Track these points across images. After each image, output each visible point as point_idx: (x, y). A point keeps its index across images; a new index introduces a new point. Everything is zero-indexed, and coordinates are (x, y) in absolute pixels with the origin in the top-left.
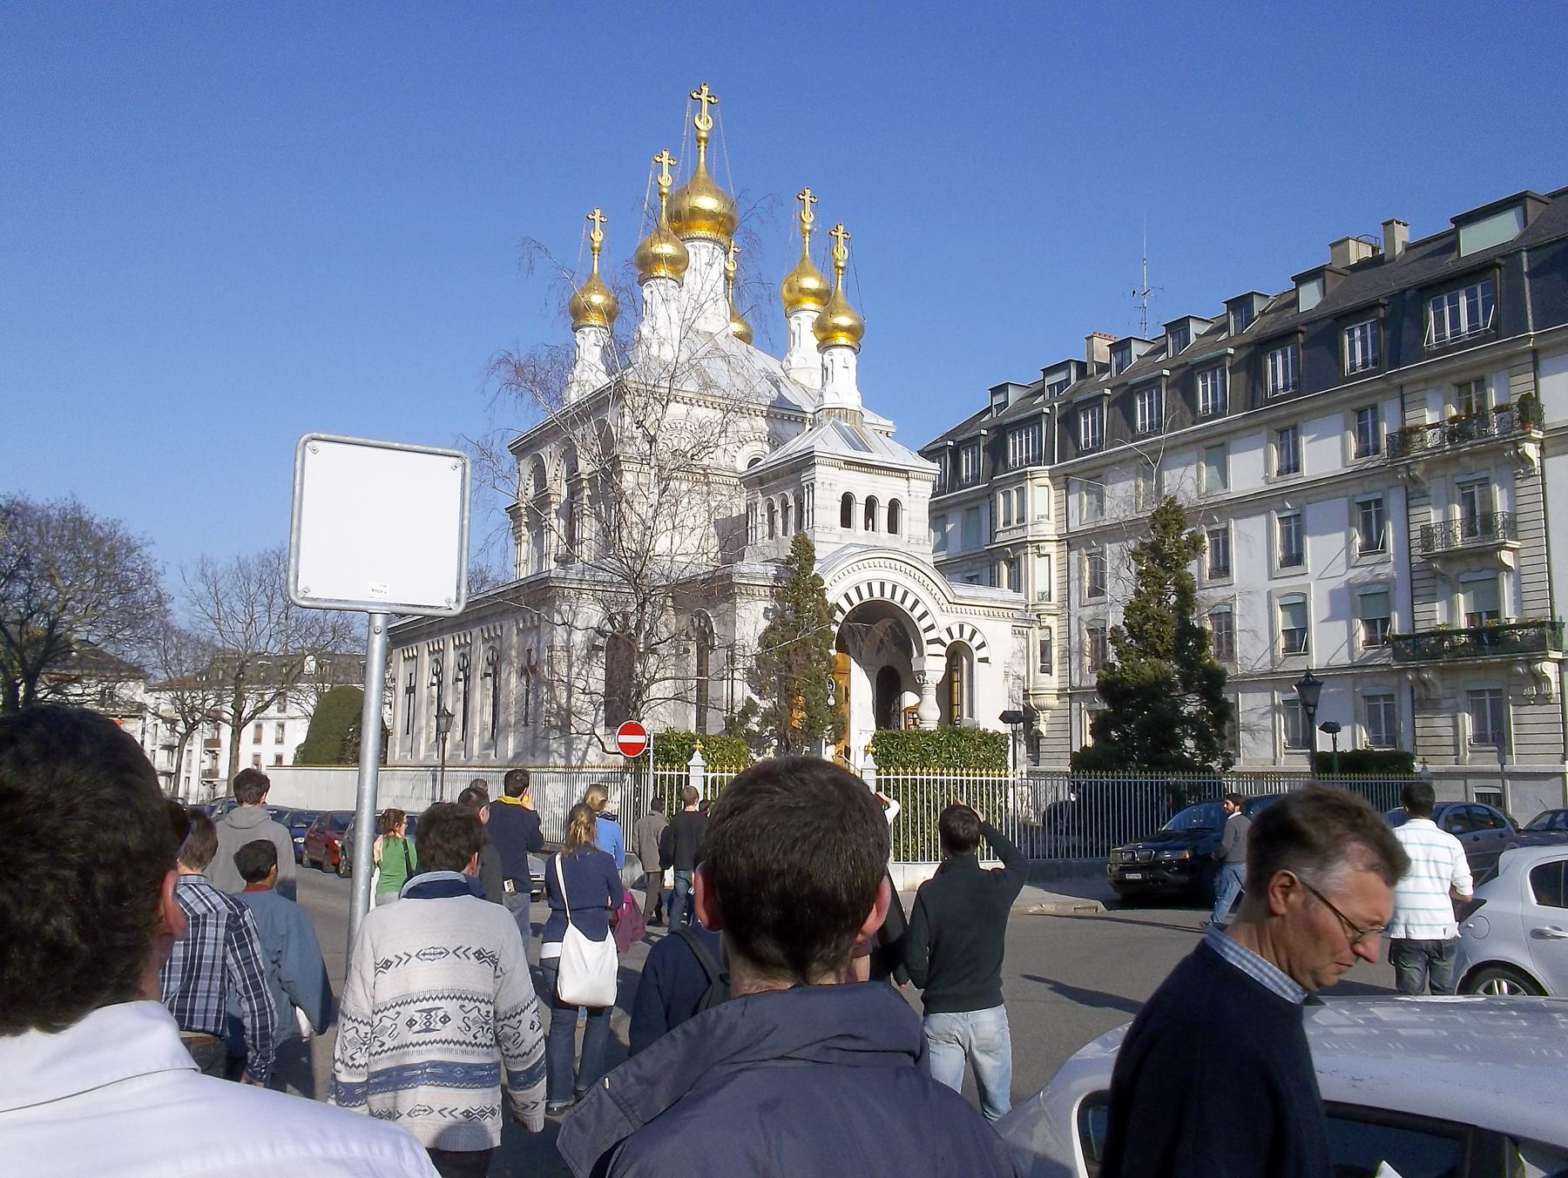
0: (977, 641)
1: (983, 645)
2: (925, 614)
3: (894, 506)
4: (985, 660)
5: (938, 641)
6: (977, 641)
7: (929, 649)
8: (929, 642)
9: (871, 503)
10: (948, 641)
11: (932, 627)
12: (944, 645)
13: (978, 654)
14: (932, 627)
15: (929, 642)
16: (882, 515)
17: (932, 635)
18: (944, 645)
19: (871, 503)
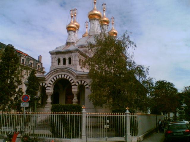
0: (85, 84)
2: (72, 80)
3: (70, 59)
4: (87, 88)
5: (75, 85)
6: (85, 84)
7: (73, 87)
10: (77, 84)
11: (73, 82)
12: (77, 86)
14: (73, 82)
16: (67, 62)
18: (77, 86)
19: (64, 60)
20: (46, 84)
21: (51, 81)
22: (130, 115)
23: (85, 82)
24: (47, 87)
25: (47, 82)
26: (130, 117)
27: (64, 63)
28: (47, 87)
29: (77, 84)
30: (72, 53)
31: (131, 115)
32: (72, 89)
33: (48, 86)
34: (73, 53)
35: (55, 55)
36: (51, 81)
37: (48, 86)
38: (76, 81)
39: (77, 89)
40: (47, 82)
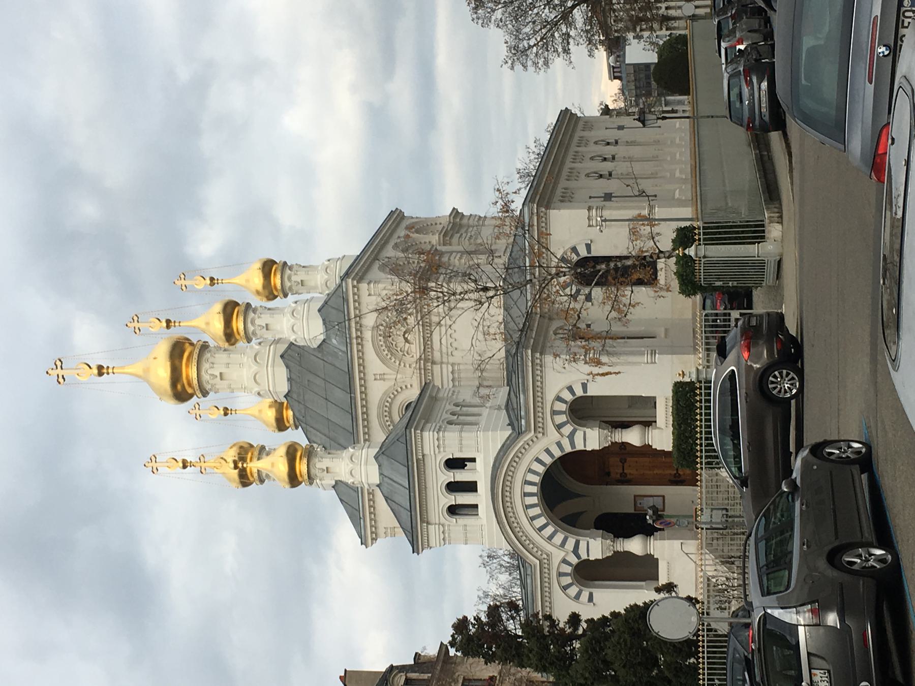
1: (570, 389)
2: (548, 451)
4: (584, 386)
5: (571, 437)
7: (580, 446)
8: (572, 444)
9: (453, 487)
10: (567, 430)
11: (559, 444)
12: (574, 431)
13: (579, 392)
14: (559, 444)
15: (572, 444)
16: (461, 476)
17: (566, 443)
18: (574, 431)
19: (453, 487)
20: (564, 561)
21: (551, 538)
22: (700, 244)
23: (559, 399)
24: (578, 557)
25: (558, 555)
26: (705, 244)
27: (471, 487)
28: (578, 557)
29: (567, 430)
30: (423, 456)
31: (699, 239)
32: (589, 449)
33: (576, 551)
34: (426, 452)
35: (431, 528)
36: (551, 538)
37: (576, 551)
38: (553, 435)
39: (588, 431)
40: (558, 555)
